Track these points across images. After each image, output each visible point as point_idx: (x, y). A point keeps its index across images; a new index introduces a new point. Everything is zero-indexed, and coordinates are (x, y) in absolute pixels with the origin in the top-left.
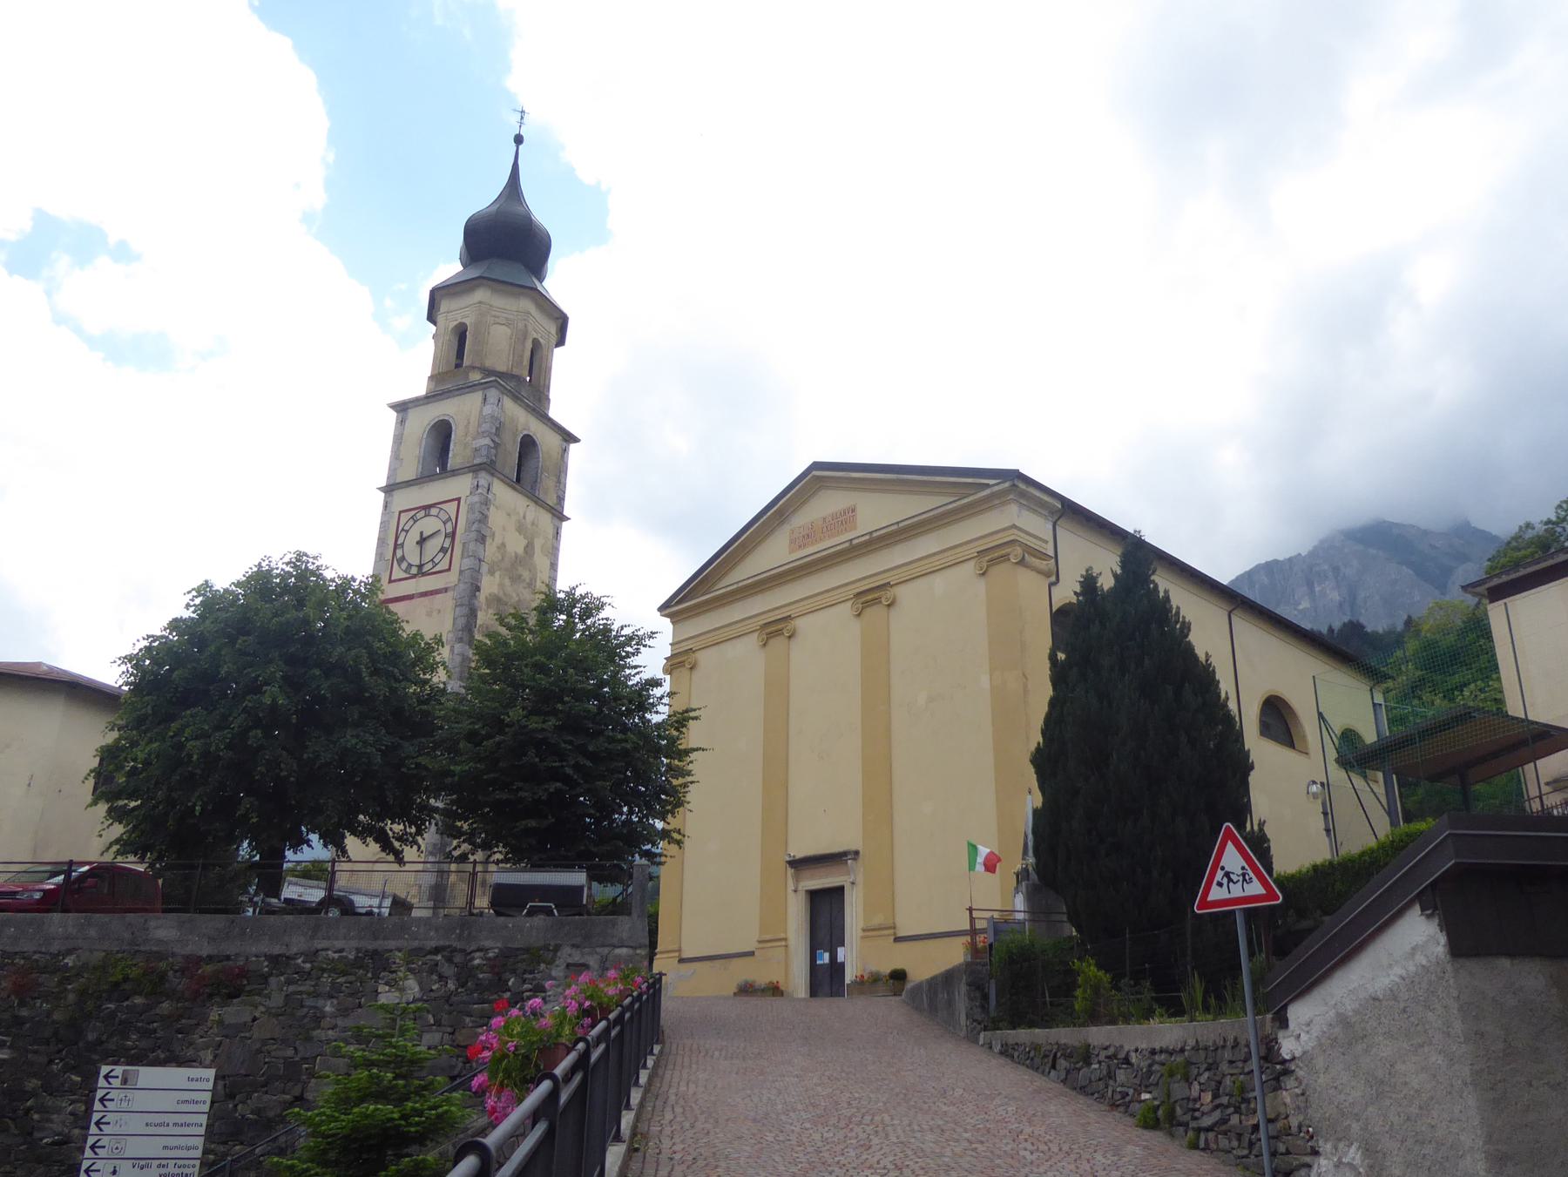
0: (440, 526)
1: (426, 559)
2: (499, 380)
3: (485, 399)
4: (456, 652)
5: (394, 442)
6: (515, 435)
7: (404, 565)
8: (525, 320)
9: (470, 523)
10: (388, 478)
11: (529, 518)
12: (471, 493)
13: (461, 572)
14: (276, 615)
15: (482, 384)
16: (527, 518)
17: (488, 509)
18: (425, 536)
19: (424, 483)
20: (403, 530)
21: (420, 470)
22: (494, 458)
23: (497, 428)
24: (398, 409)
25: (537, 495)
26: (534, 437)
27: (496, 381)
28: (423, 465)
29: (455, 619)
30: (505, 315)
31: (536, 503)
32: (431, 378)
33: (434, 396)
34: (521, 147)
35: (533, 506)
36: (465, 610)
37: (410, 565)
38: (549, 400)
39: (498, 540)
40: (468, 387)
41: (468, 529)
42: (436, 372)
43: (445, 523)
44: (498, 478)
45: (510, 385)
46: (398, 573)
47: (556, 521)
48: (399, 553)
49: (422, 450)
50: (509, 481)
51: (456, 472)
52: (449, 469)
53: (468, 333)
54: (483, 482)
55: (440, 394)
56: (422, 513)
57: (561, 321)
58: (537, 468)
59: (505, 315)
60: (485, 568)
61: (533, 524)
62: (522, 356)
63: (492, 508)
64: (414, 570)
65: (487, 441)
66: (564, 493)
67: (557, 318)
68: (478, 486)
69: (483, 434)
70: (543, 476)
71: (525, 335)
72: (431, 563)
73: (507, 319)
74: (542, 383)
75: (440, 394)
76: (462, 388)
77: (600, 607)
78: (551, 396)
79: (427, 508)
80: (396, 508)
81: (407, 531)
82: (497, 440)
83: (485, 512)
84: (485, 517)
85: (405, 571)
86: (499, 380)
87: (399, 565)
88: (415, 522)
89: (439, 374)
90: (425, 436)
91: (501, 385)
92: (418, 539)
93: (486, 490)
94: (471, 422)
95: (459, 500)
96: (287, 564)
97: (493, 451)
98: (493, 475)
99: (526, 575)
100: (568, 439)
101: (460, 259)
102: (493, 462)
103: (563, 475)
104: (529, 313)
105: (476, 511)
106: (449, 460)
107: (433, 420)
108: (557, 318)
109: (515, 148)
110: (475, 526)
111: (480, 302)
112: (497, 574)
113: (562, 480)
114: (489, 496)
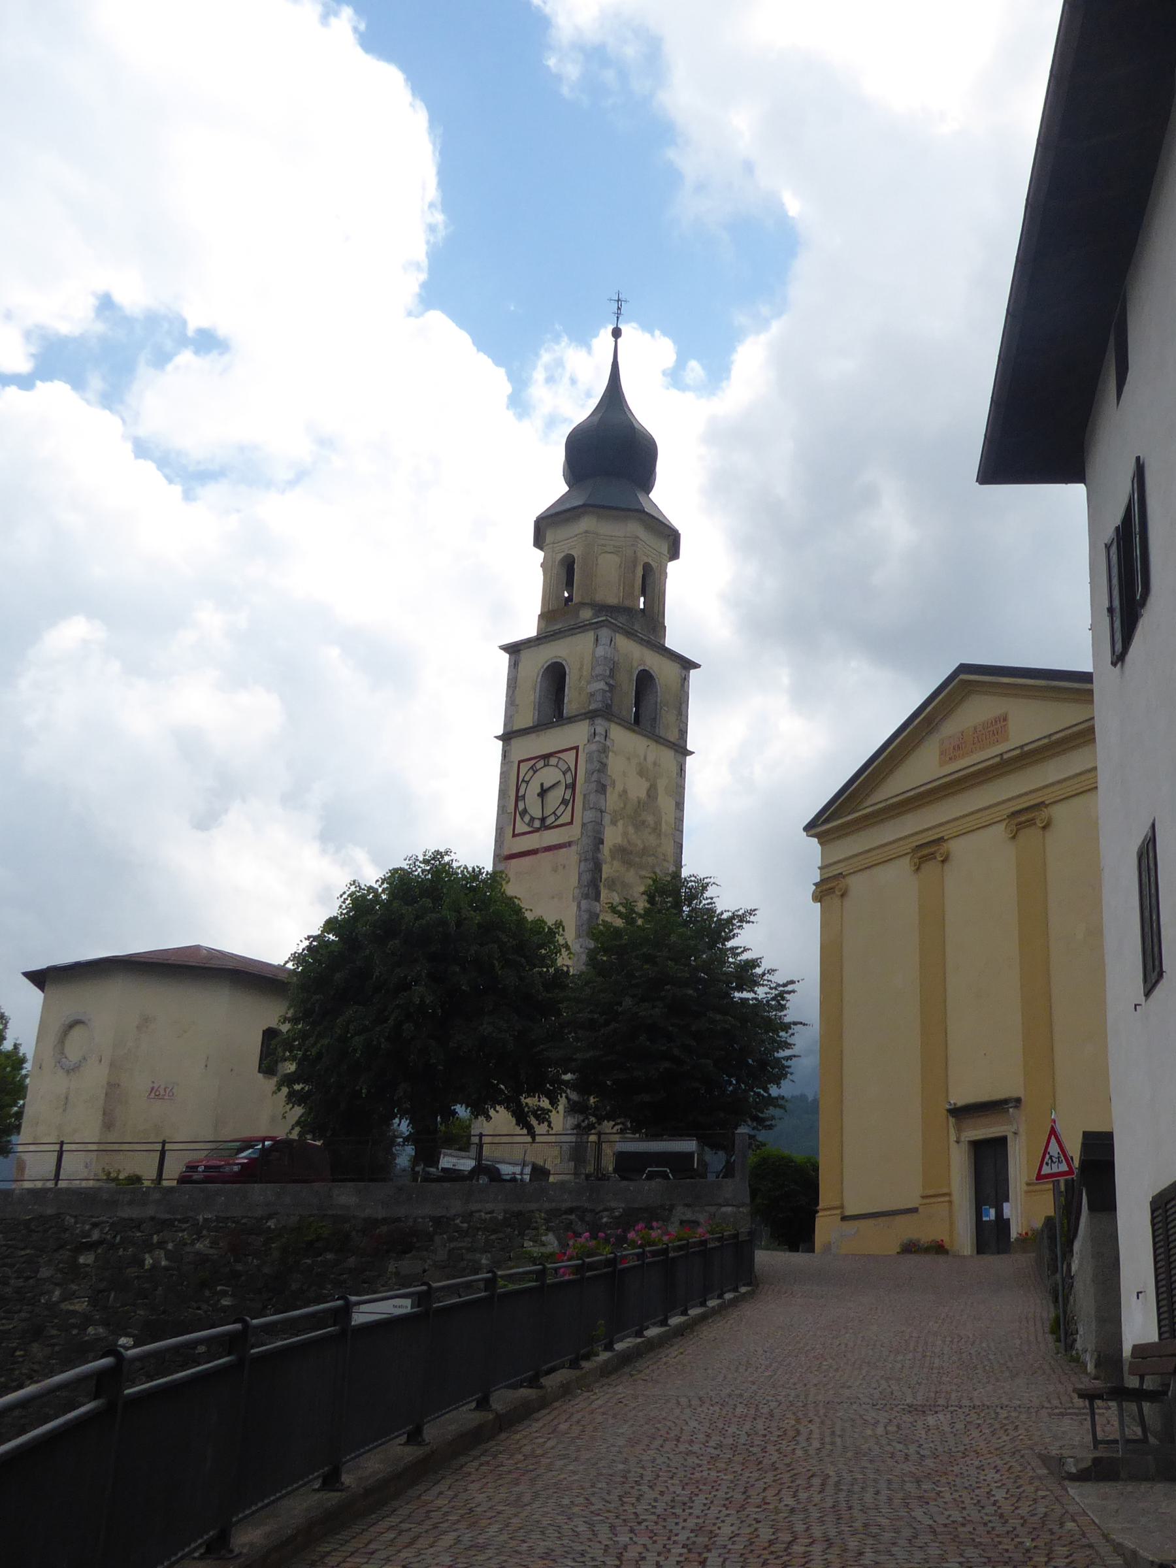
0: (561, 777)
1: (548, 812)
4: (583, 908)
5: (509, 686)
7: (527, 819)
8: (633, 545)
9: (589, 774)
11: (651, 758)
12: (588, 741)
13: (583, 825)
14: (417, 918)
17: (607, 757)
18: (545, 787)
19: (542, 730)
20: (523, 781)
21: (536, 717)
23: (611, 670)
26: (652, 672)
27: (607, 620)
28: (539, 711)
29: (580, 874)
31: (656, 741)
32: (542, 617)
34: (619, 340)
35: (653, 745)
36: (591, 865)
37: (532, 819)
39: (619, 787)
40: (580, 627)
41: (587, 780)
42: (546, 610)
43: (564, 773)
44: (616, 723)
45: (622, 620)
46: (521, 827)
48: (521, 806)
51: (573, 720)
52: (565, 715)
53: (575, 566)
55: (552, 635)
56: (541, 763)
59: (612, 543)
60: (607, 819)
61: (655, 764)
62: (633, 586)
64: (537, 824)
65: (601, 685)
68: (595, 733)
69: (595, 678)
70: (663, 711)
72: (553, 816)
73: (614, 546)
76: (573, 629)
77: (705, 887)
79: (546, 757)
80: (516, 757)
81: (527, 782)
82: (611, 682)
83: (604, 760)
85: (528, 825)
87: (522, 819)
88: (535, 772)
90: (539, 680)
91: (612, 623)
92: (539, 790)
93: (603, 737)
95: (577, 748)
97: (609, 694)
98: (609, 720)
99: (650, 820)
102: (608, 707)
103: (684, 706)
107: (546, 662)
110: (595, 777)
111: (586, 532)
112: (620, 823)
114: (608, 743)
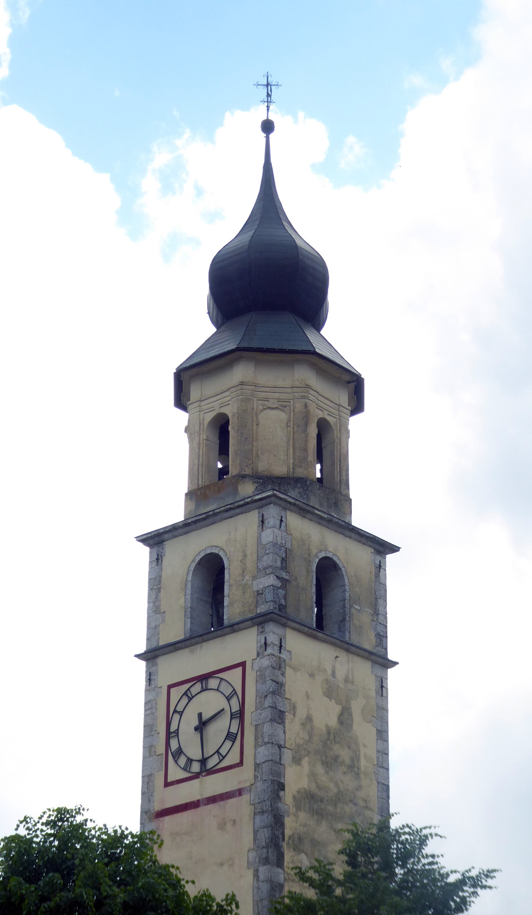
0: (223, 703)
1: (210, 750)
2: (278, 494)
3: (263, 522)
4: (262, 877)
5: (151, 589)
6: (309, 562)
7: (182, 761)
8: (303, 397)
9: (262, 697)
10: (148, 639)
11: (341, 673)
12: (258, 655)
13: (257, 766)
14: (43, 899)
15: (256, 501)
16: (337, 673)
17: (283, 674)
18: (205, 717)
19: (197, 643)
20: (175, 711)
21: (188, 625)
22: (283, 601)
23: (283, 560)
24: (151, 542)
25: (347, 639)
26: (335, 559)
27: (274, 495)
28: (192, 618)
29: (255, 832)
30: (276, 395)
31: (347, 650)
32: (190, 495)
33: (195, 522)
34: (271, 136)
35: (343, 656)
36: (267, 819)
37: (190, 761)
38: (351, 500)
39: (301, 713)
40: (239, 507)
41: (259, 706)
42: (195, 487)
43: (228, 699)
44: (293, 629)
45: (294, 494)
46: (175, 773)
47: (378, 670)
48: (174, 744)
49: (189, 597)
50: (306, 629)
51: (236, 627)
52: (226, 622)
53: (230, 428)
54: (272, 638)
55: (204, 519)
56: (198, 687)
57: (352, 385)
58: (344, 600)
59: (276, 395)
60: (287, 756)
61: (346, 680)
62: (305, 450)
63: (289, 671)
64: (196, 767)
65: (271, 580)
66: (386, 627)
67: (349, 382)
68: (265, 643)
69: (264, 571)
70: (353, 610)
71: (306, 416)
72: (216, 756)
73: (279, 400)
74: (337, 479)
75: (204, 519)
76: (231, 509)
77: (423, 841)
78: (353, 494)
79: (204, 678)
80: (164, 681)
81: (181, 713)
82: (284, 575)
83: (280, 679)
84: (280, 685)
85: (185, 769)
86: (278, 494)
87: (176, 762)
88: (190, 699)
89: (199, 489)
90: (190, 578)
91: (281, 499)
92: (196, 723)
93: (277, 648)
94: (248, 553)
95: (243, 664)
96: (47, 824)
97: (281, 592)
98: (284, 625)
99: (344, 754)
100: (381, 549)
101: (209, 313)
102: (282, 608)
103: (380, 601)
104: (308, 386)
105: (268, 678)
106: (225, 610)
107: (198, 554)
108: (349, 382)
109: (264, 140)
110: (268, 702)
111: (242, 383)
112: (305, 761)
113: (381, 609)
114: (282, 656)
